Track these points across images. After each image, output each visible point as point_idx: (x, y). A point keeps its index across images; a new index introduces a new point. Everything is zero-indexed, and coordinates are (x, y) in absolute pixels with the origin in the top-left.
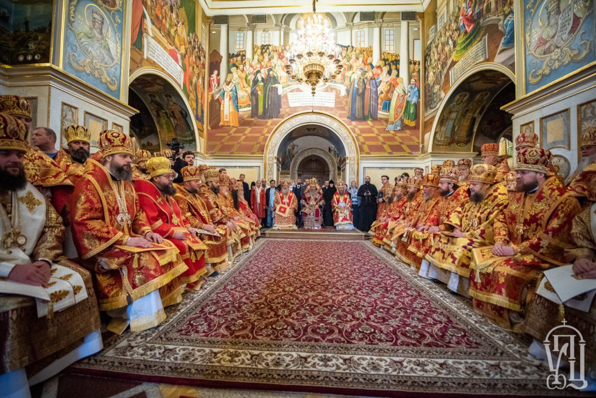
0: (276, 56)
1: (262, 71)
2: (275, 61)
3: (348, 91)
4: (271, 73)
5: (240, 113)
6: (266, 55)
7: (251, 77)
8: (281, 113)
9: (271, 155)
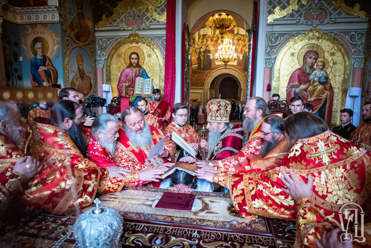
0: (209, 39)
1: (203, 47)
2: (209, 42)
3: (243, 57)
4: (207, 48)
5: (193, 68)
6: (205, 40)
7: (198, 51)
8: (212, 67)
9: (207, 88)
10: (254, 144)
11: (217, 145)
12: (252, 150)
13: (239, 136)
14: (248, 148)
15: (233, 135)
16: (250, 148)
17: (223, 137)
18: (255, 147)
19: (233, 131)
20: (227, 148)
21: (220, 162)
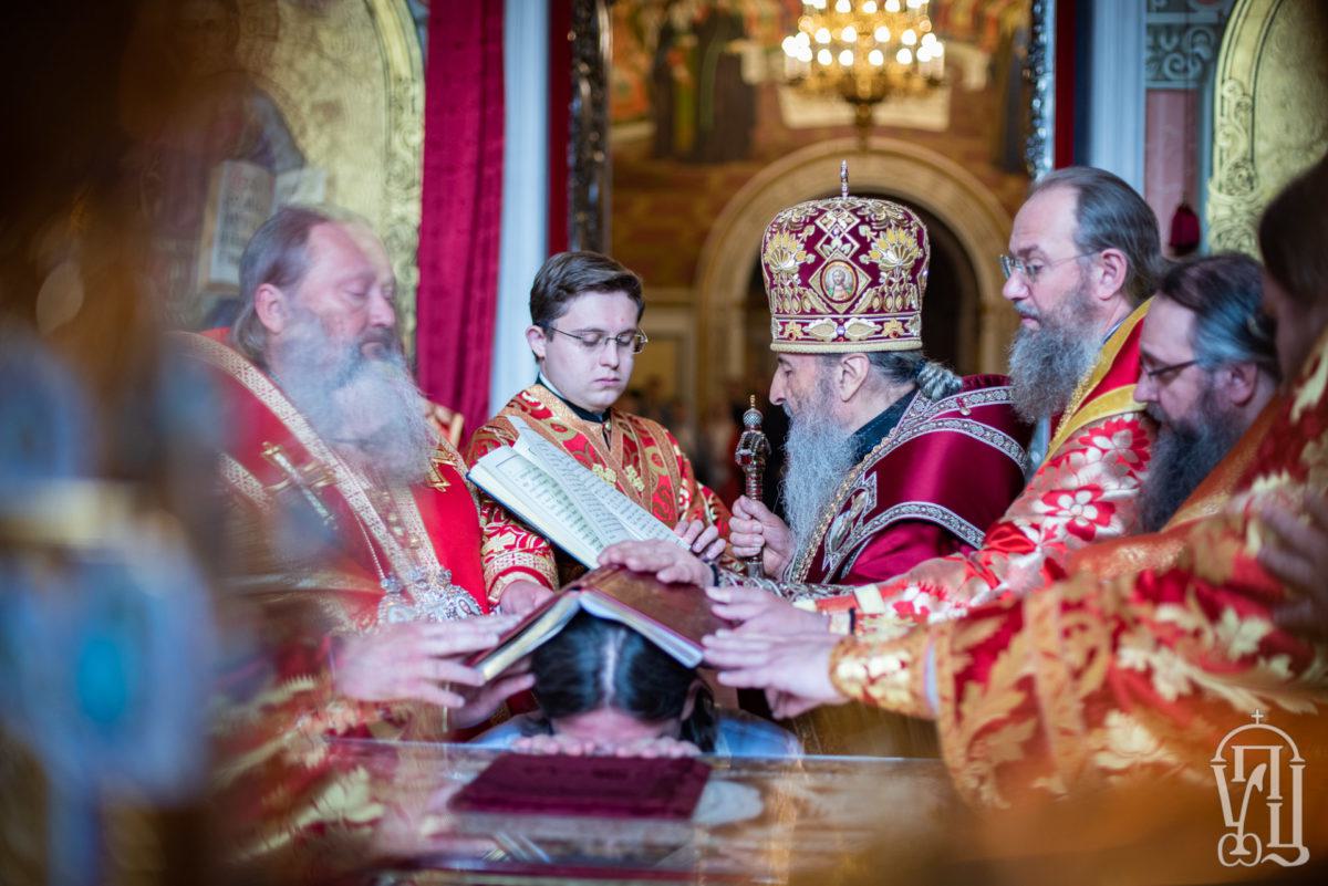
10: (1091, 465)
11: (847, 506)
12: (1076, 510)
13: (996, 439)
14: (1051, 497)
15: (953, 426)
16: (1064, 500)
17: (882, 449)
18: (1095, 489)
19: (955, 407)
20: (910, 509)
21: (868, 596)
